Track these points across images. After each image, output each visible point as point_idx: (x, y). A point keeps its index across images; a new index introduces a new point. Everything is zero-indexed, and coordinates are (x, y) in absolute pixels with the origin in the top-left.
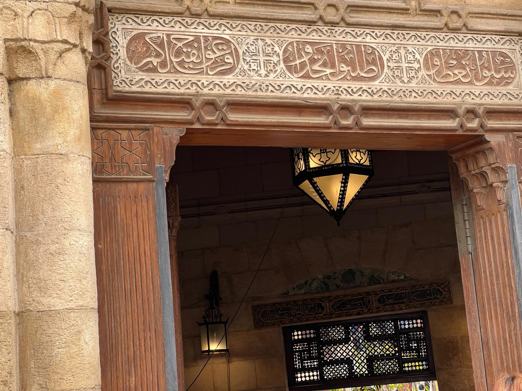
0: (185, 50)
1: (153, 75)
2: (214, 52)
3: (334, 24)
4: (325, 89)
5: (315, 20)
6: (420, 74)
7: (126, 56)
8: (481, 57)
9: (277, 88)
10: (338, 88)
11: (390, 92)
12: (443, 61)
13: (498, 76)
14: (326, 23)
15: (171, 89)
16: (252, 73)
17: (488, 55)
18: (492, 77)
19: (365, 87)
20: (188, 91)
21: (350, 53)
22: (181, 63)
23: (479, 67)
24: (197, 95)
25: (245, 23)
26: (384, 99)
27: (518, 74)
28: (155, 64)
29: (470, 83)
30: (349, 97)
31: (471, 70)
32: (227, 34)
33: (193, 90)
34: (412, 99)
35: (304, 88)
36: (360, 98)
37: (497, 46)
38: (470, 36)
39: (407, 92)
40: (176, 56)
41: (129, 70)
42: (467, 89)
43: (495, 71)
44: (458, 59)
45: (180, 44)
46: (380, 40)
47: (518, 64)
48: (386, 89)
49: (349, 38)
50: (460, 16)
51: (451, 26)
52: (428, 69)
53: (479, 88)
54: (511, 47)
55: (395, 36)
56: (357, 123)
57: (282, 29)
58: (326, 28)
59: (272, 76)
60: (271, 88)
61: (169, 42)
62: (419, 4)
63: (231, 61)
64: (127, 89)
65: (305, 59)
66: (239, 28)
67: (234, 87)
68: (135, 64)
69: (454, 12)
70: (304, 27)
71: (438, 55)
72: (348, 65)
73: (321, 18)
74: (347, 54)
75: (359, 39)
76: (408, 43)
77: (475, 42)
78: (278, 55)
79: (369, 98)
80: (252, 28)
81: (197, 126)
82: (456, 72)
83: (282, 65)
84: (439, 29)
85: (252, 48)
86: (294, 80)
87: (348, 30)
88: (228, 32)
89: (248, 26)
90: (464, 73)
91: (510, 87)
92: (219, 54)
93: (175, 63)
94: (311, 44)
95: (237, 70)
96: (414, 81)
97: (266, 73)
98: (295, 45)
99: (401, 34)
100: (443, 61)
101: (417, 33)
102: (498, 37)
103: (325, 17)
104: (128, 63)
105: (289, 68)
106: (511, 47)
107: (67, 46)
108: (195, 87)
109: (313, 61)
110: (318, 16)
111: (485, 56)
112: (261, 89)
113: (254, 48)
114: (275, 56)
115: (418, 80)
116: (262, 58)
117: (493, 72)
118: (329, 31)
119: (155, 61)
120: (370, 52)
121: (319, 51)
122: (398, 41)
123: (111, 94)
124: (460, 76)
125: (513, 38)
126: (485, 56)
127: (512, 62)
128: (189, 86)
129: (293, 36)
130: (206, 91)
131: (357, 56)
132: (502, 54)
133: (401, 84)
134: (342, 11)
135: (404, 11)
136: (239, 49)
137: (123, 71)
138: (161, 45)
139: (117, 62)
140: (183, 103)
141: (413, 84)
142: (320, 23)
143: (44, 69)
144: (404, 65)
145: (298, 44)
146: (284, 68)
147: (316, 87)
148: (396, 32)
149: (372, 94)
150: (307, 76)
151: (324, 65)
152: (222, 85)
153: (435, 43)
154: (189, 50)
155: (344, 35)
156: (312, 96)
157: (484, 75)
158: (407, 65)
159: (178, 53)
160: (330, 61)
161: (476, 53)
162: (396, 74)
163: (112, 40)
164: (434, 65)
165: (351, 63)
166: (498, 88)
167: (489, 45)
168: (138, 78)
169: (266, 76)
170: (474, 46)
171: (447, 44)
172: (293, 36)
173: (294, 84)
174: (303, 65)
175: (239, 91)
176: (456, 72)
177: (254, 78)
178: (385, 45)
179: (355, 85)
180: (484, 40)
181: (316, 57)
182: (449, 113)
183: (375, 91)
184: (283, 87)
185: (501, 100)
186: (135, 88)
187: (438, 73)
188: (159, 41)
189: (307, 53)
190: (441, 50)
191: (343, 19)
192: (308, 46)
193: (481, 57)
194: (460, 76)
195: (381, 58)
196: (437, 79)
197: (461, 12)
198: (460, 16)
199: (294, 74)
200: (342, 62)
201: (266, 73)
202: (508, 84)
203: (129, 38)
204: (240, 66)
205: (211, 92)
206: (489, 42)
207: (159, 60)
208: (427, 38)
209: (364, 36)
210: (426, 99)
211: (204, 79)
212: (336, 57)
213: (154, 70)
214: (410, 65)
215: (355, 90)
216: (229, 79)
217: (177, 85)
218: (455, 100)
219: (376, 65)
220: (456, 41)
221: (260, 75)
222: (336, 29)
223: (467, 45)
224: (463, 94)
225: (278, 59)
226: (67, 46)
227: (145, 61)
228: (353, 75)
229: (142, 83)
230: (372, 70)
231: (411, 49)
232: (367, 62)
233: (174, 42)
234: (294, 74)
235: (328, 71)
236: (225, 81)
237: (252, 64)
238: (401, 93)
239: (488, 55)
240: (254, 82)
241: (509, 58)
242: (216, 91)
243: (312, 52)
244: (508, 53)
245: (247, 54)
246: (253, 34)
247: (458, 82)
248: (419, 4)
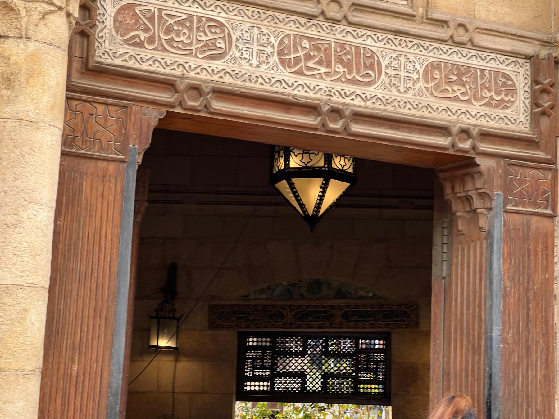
0: (176, 28)
1: (138, 50)
2: (206, 34)
3: (335, 21)
4: (317, 88)
5: (316, 14)
6: (418, 86)
7: (112, 26)
8: (483, 76)
9: (267, 81)
10: (330, 89)
11: (384, 100)
12: (443, 75)
13: (498, 98)
14: (328, 19)
15: (156, 68)
16: (243, 62)
17: (490, 74)
18: (492, 98)
19: (359, 92)
20: (173, 72)
21: (348, 54)
22: (170, 42)
23: (479, 86)
24: (182, 77)
25: (242, 7)
26: (377, 107)
27: (518, 99)
28: (142, 39)
29: (468, 101)
30: (341, 100)
31: (471, 88)
33: (179, 71)
34: (406, 111)
35: (296, 84)
36: (352, 102)
37: (501, 66)
38: (474, 52)
39: (402, 102)
40: (166, 33)
41: (114, 42)
42: (464, 107)
43: (495, 93)
44: (460, 75)
45: (171, 21)
46: (381, 44)
47: (520, 89)
48: (380, 96)
49: (349, 38)
50: (467, 30)
51: (456, 39)
52: (427, 81)
53: (476, 108)
54: (515, 69)
55: (397, 43)
56: (346, 128)
57: (281, 19)
58: (327, 24)
59: (264, 67)
60: (260, 80)
61: (160, 18)
62: (427, 11)
63: (222, 46)
64: (109, 61)
65: (301, 54)
66: (235, 12)
67: (222, 74)
68: (121, 36)
69: (461, 25)
70: (304, 20)
71: (439, 68)
72: (344, 67)
73: (323, 13)
74: (345, 54)
75: (360, 40)
76: (409, 51)
77: (479, 59)
78: (273, 46)
79: (362, 103)
80: (249, 14)
81: (178, 110)
82: (455, 88)
83: (276, 57)
84: (443, 41)
85: (246, 35)
86: (286, 74)
87: (350, 29)
88: (223, 14)
89: (246, 11)
91: (509, 111)
92: (211, 37)
93: (163, 41)
94: (309, 39)
95: (228, 57)
96: (411, 92)
97: (258, 63)
98: (292, 38)
99: (403, 41)
100: (443, 75)
101: (421, 42)
102: (504, 57)
103: (327, 13)
104: (114, 33)
105: (283, 62)
106: (515, 69)
107: (52, 8)
108: (181, 69)
109: (308, 57)
110: (320, 11)
111: (487, 75)
112: (250, 80)
113: (248, 35)
114: (269, 47)
115: (415, 91)
116: (255, 47)
117: (493, 93)
118: (330, 28)
119: (143, 36)
120: (369, 55)
121: (317, 48)
122: (399, 48)
123: (91, 64)
124: (458, 93)
125: (519, 60)
126: (487, 75)
127: (514, 85)
128: (175, 67)
129: (291, 28)
130: (192, 74)
131: (355, 58)
132: (506, 76)
133: (397, 94)
134: (345, 8)
135: (410, 17)
136: (232, 35)
137: (107, 42)
138: (151, 19)
139: (102, 31)
140: (168, 84)
141: (409, 95)
142: (321, 18)
143: (24, 28)
144: (403, 74)
145: (295, 38)
146: (278, 61)
147: (308, 85)
148: (399, 38)
149: (366, 100)
150: (299, 73)
151: (320, 63)
152: (209, 70)
153: (437, 55)
154: (180, 29)
155: (344, 34)
156: (303, 93)
157: (484, 95)
158: (406, 74)
159: (168, 30)
160: (326, 59)
161: (478, 71)
162: (393, 82)
163: (100, 7)
165: (348, 65)
166: (496, 110)
167: (493, 64)
168: (122, 51)
169: (258, 66)
170: (477, 63)
171: (449, 58)
173: (286, 79)
174: (297, 60)
175: (227, 79)
176: (455, 88)
177: (244, 67)
178: (386, 50)
179: (349, 88)
180: (488, 58)
181: (312, 54)
182: (442, 130)
183: (369, 97)
184: (273, 80)
185: (498, 124)
186: (117, 62)
187: (437, 86)
188: (149, 15)
190: (442, 64)
191: (345, 17)
192: (305, 41)
193: (483, 76)
194: (458, 93)
195: (379, 63)
196: (434, 93)
197: (469, 27)
198: (467, 30)
199: (287, 68)
200: (338, 62)
201: (258, 63)
202: (507, 107)
203: (118, 7)
204: (231, 53)
205: (198, 76)
206: (493, 61)
207: (147, 35)
208: (431, 48)
209: (365, 38)
210: (420, 113)
211: (192, 62)
212: (333, 56)
213: (140, 45)
214: (409, 75)
215: (348, 93)
216: (218, 65)
217: (163, 64)
218: (450, 118)
219: (373, 70)
220: (460, 55)
221: (251, 65)
222: (337, 26)
223: (470, 61)
224: (459, 112)
225: (272, 50)
226: (52, 8)
227: (132, 34)
228: (348, 77)
229: (126, 57)
230: (369, 75)
231: (411, 58)
232: (365, 65)
233: (166, 18)
234: (287, 68)
235: (323, 70)
236: (214, 67)
237: (245, 53)
238: (396, 103)
239: (490, 74)
240: (244, 72)
241: (512, 80)
242: (203, 76)
243: (308, 47)
244: (511, 75)
245: (241, 41)
246: (249, 20)
247: (455, 99)
248: (427, 11)
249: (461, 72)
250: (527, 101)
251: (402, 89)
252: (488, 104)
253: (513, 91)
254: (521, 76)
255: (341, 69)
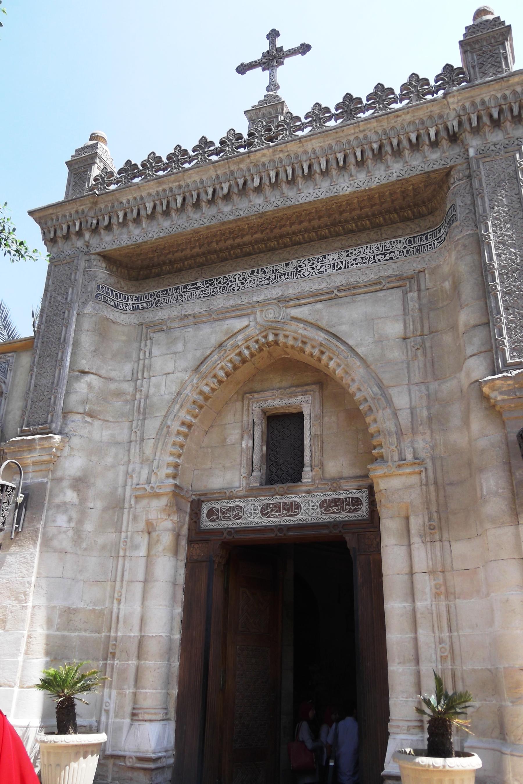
1: (214, 522)
6: (316, 511)
14: (279, 495)
18: (350, 508)
22: (223, 517)
29: (340, 512)
30: (285, 523)
31: (341, 507)
32: (241, 504)
33: (226, 526)
34: (312, 522)
40: (223, 514)
52: (321, 508)
59: (256, 518)
61: (221, 510)
70: (270, 497)
71: (326, 502)
79: (293, 523)
82: (333, 508)
86: (264, 519)
87: (288, 496)
90: (337, 508)
92: (237, 512)
94: (272, 504)
96: (314, 514)
102: (355, 491)
105: (262, 515)
109: (272, 511)
116: (252, 512)
119: (215, 517)
121: (275, 507)
127: (361, 501)
130: (231, 526)
138: (218, 512)
150: (269, 517)
151: (277, 512)
164: (324, 507)
165: (288, 510)
172: (266, 502)
174: (268, 513)
175: (243, 526)
179: (287, 519)
187: (325, 510)
189: (270, 508)
202: (358, 511)
213: (214, 521)
231: (314, 501)
235: (278, 514)
247: (334, 512)
249: (336, 502)
250: (367, 507)
251: (310, 514)
252: (349, 512)
253: (362, 504)
254: (363, 496)
255: (285, 512)
